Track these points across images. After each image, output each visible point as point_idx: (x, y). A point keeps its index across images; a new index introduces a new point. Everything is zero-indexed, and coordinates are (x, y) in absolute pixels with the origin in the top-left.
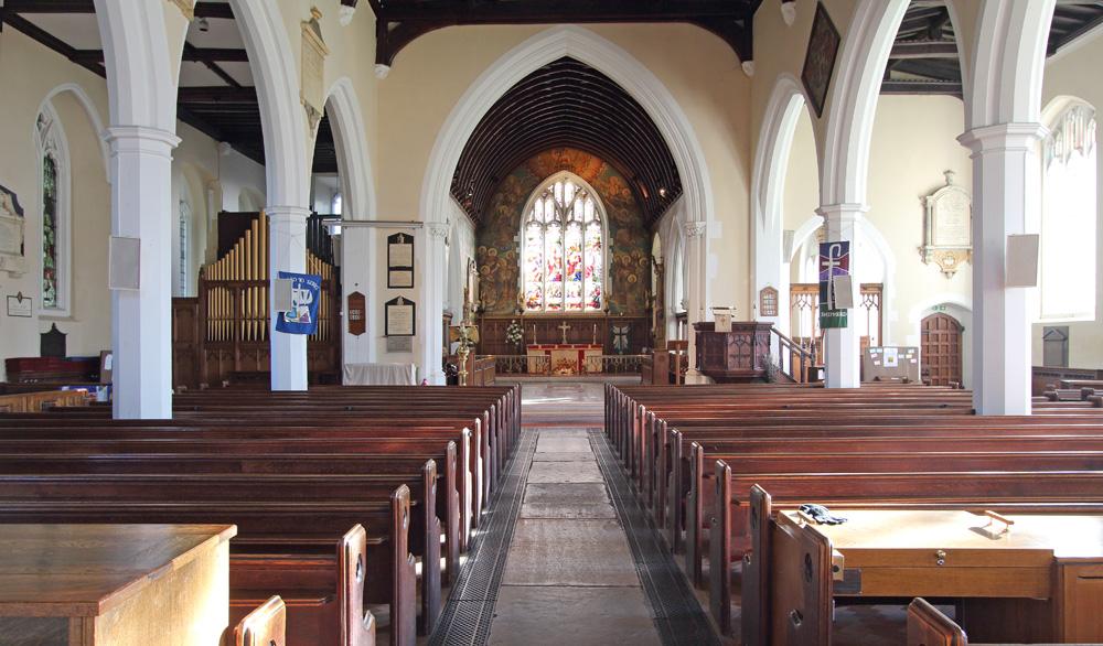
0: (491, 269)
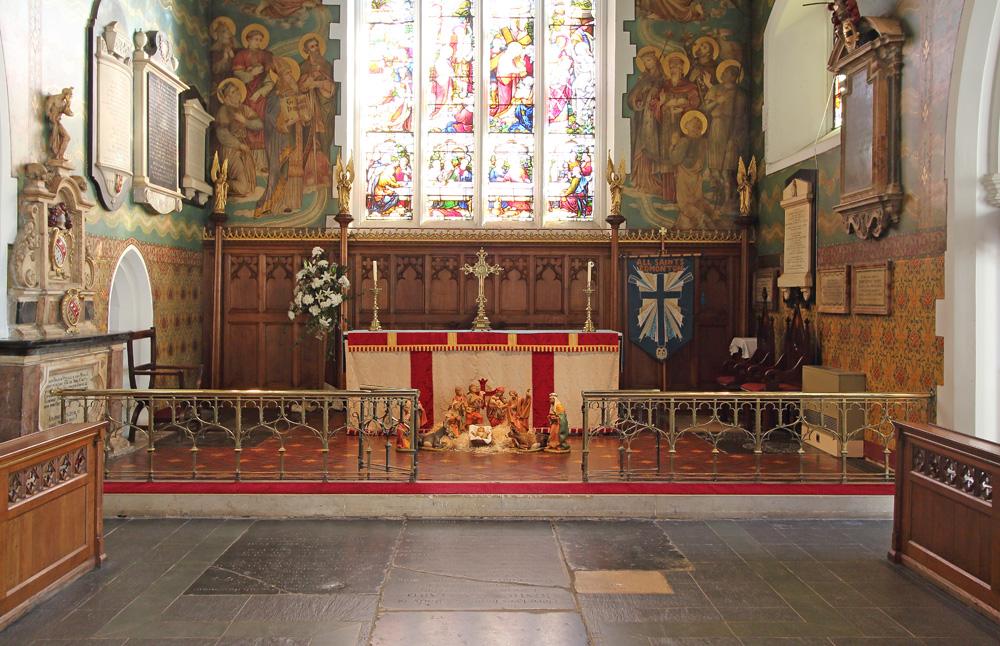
0: (251, 88)
